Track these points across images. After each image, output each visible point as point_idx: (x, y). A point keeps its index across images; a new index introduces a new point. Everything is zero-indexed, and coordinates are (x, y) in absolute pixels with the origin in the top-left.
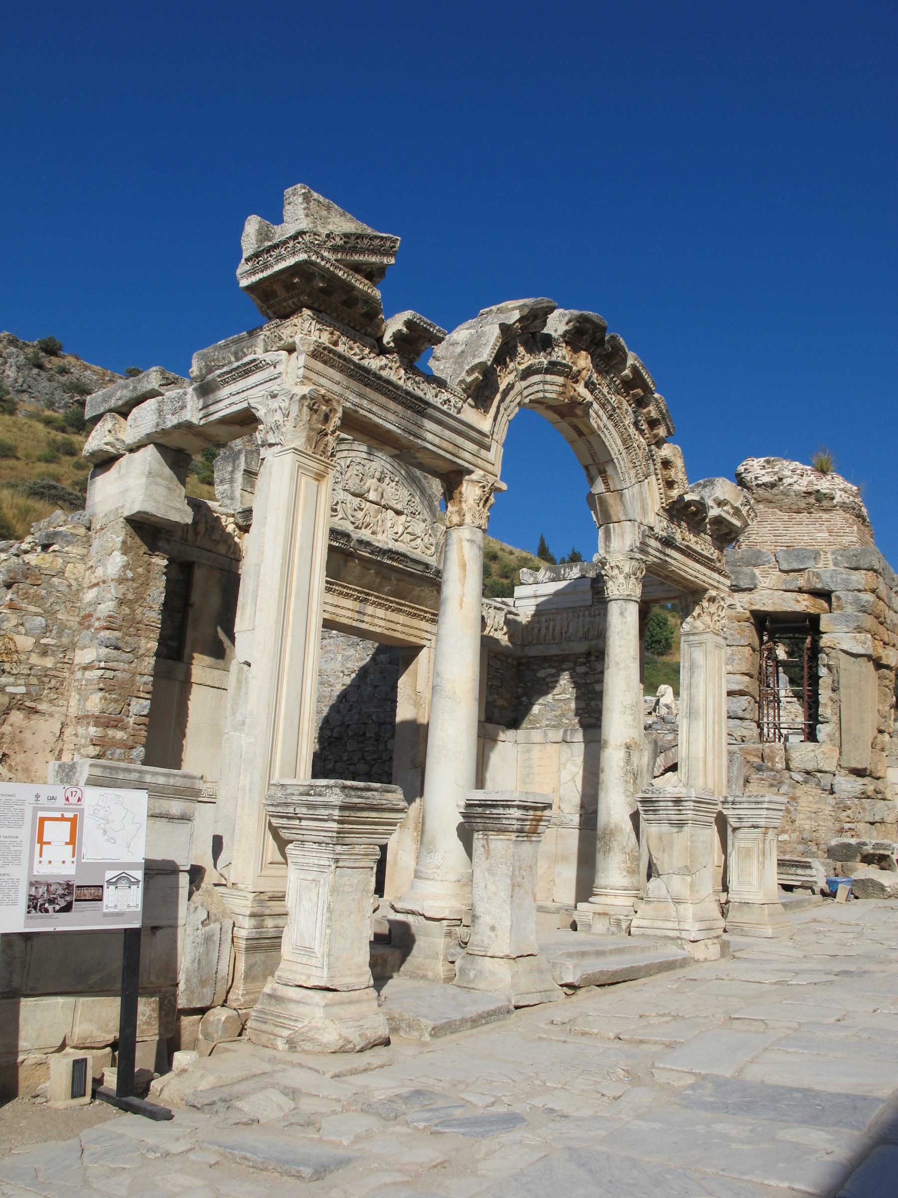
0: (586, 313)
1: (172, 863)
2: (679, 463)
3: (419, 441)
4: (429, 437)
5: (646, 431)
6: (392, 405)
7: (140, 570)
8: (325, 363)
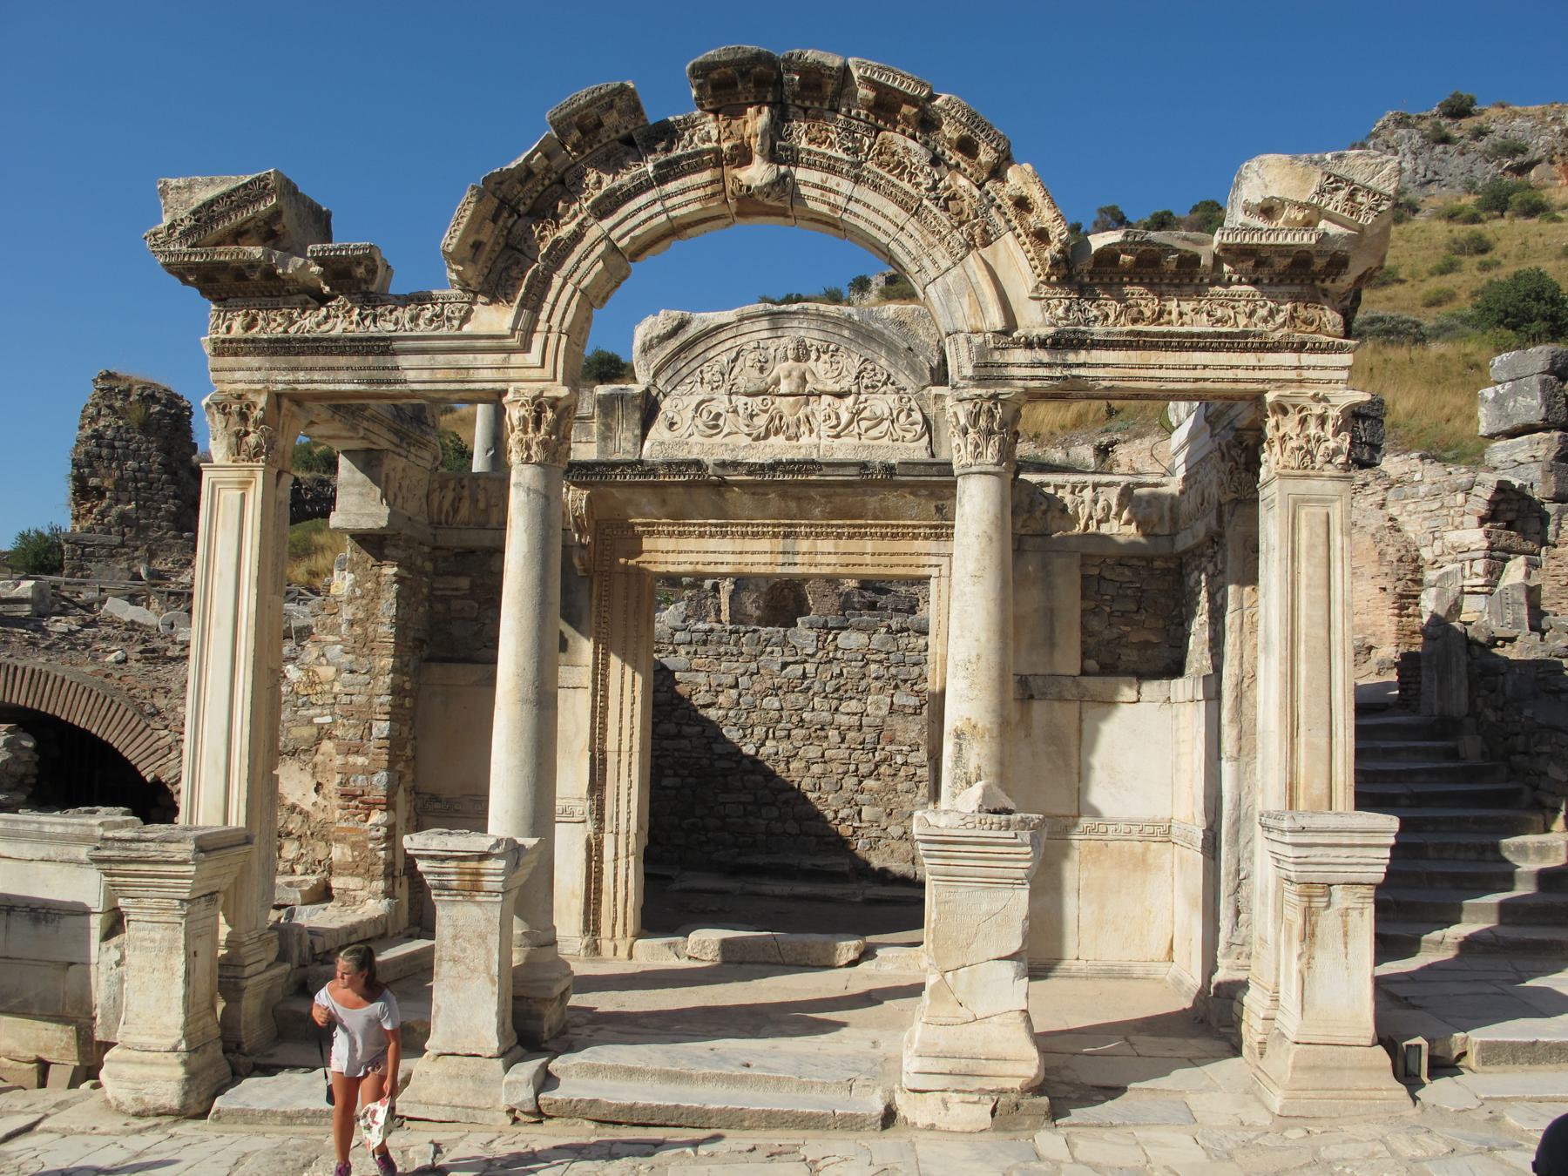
0: (700, 59)
1: (83, 905)
2: (1035, 193)
3: (398, 387)
4: (411, 375)
5: (963, 165)
6: (342, 361)
7: (369, 585)
8: (236, 354)
